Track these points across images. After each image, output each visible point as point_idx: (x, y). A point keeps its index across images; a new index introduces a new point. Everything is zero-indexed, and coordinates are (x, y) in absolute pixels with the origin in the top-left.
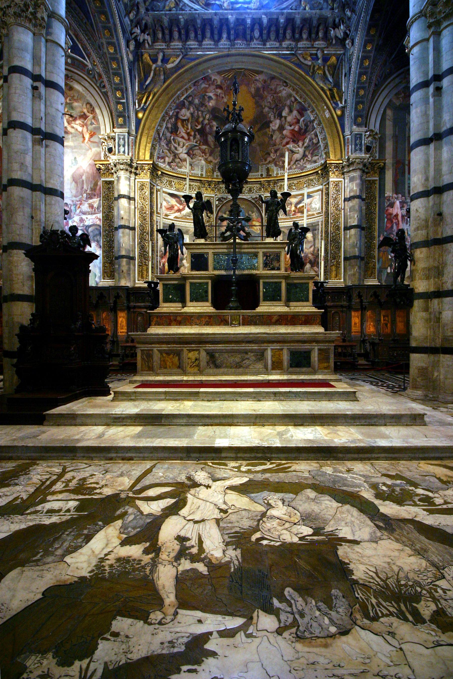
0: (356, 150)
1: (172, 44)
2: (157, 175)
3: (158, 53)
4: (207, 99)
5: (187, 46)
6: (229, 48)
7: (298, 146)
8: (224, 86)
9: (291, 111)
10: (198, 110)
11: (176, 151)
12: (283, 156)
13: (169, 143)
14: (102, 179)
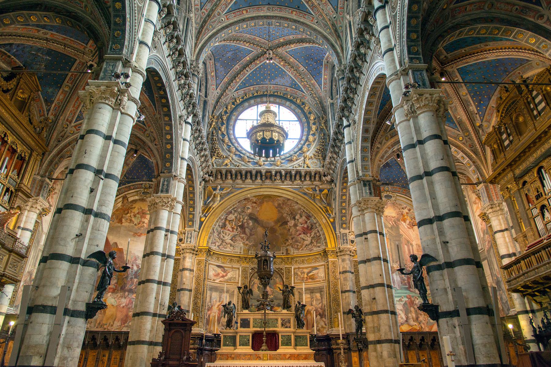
3: (217, 186)
8: (258, 203)
9: (301, 216)
10: (240, 214)
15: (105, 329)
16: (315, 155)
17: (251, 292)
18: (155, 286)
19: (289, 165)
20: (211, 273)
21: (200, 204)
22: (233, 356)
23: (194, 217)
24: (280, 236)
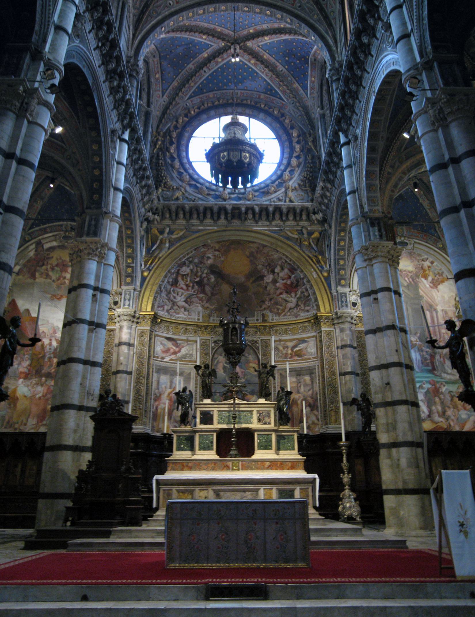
1: (177, 221)
3: (165, 228)
7: (291, 296)
9: (282, 269)
11: (175, 300)
15: (16, 429)
16: (300, 185)
17: (213, 374)
18: (80, 367)
19: (264, 199)
20: (159, 348)
21: (141, 253)
22: (190, 464)
23: (133, 271)
24: (253, 296)
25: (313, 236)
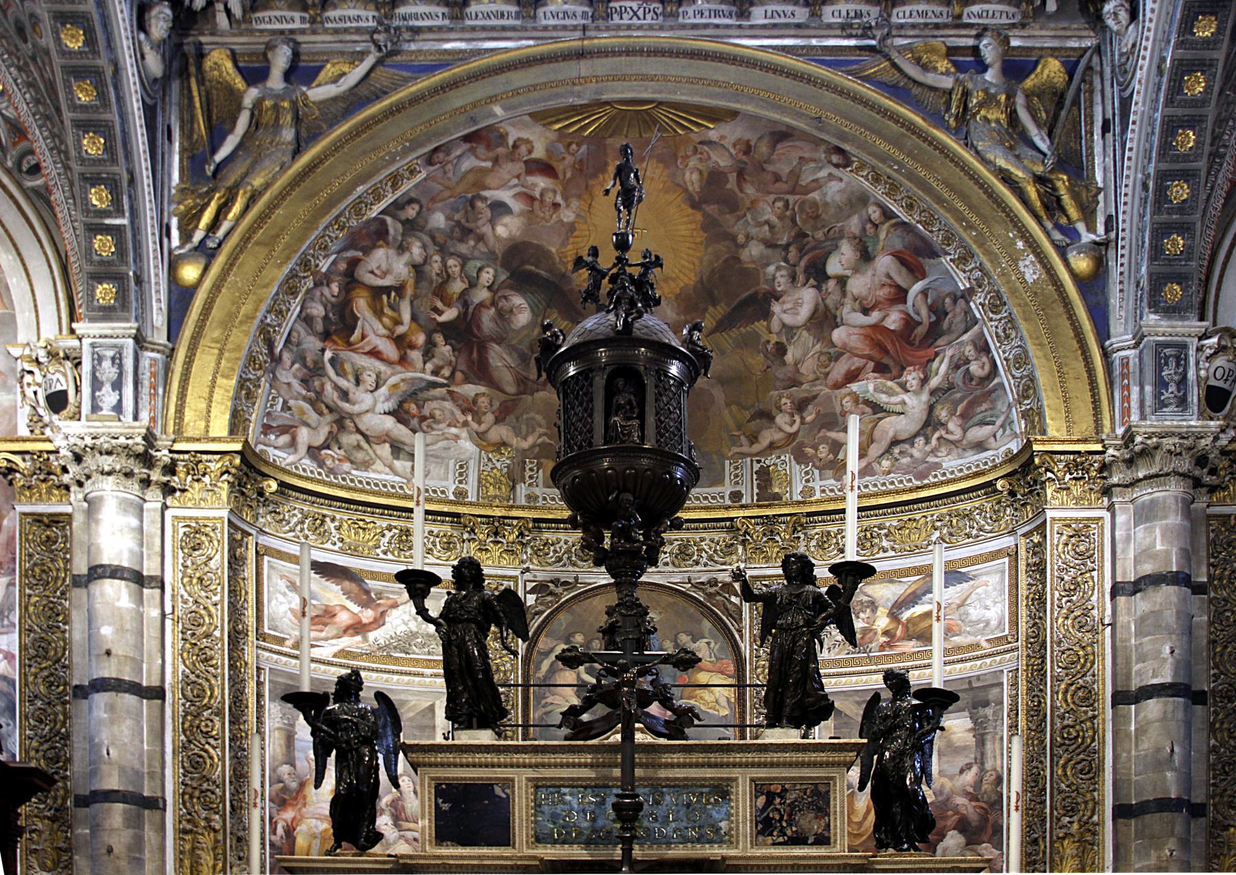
0: (1160, 405)
1: (331, 14)
2: (261, 493)
4: (488, 213)
5: (396, 23)
6: (585, 28)
8: (565, 166)
10: (443, 250)
11: (346, 406)
12: (835, 422)
13: (311, 373)
14: (20, 508)
24: (718, 394)
25: (1029, 83)
